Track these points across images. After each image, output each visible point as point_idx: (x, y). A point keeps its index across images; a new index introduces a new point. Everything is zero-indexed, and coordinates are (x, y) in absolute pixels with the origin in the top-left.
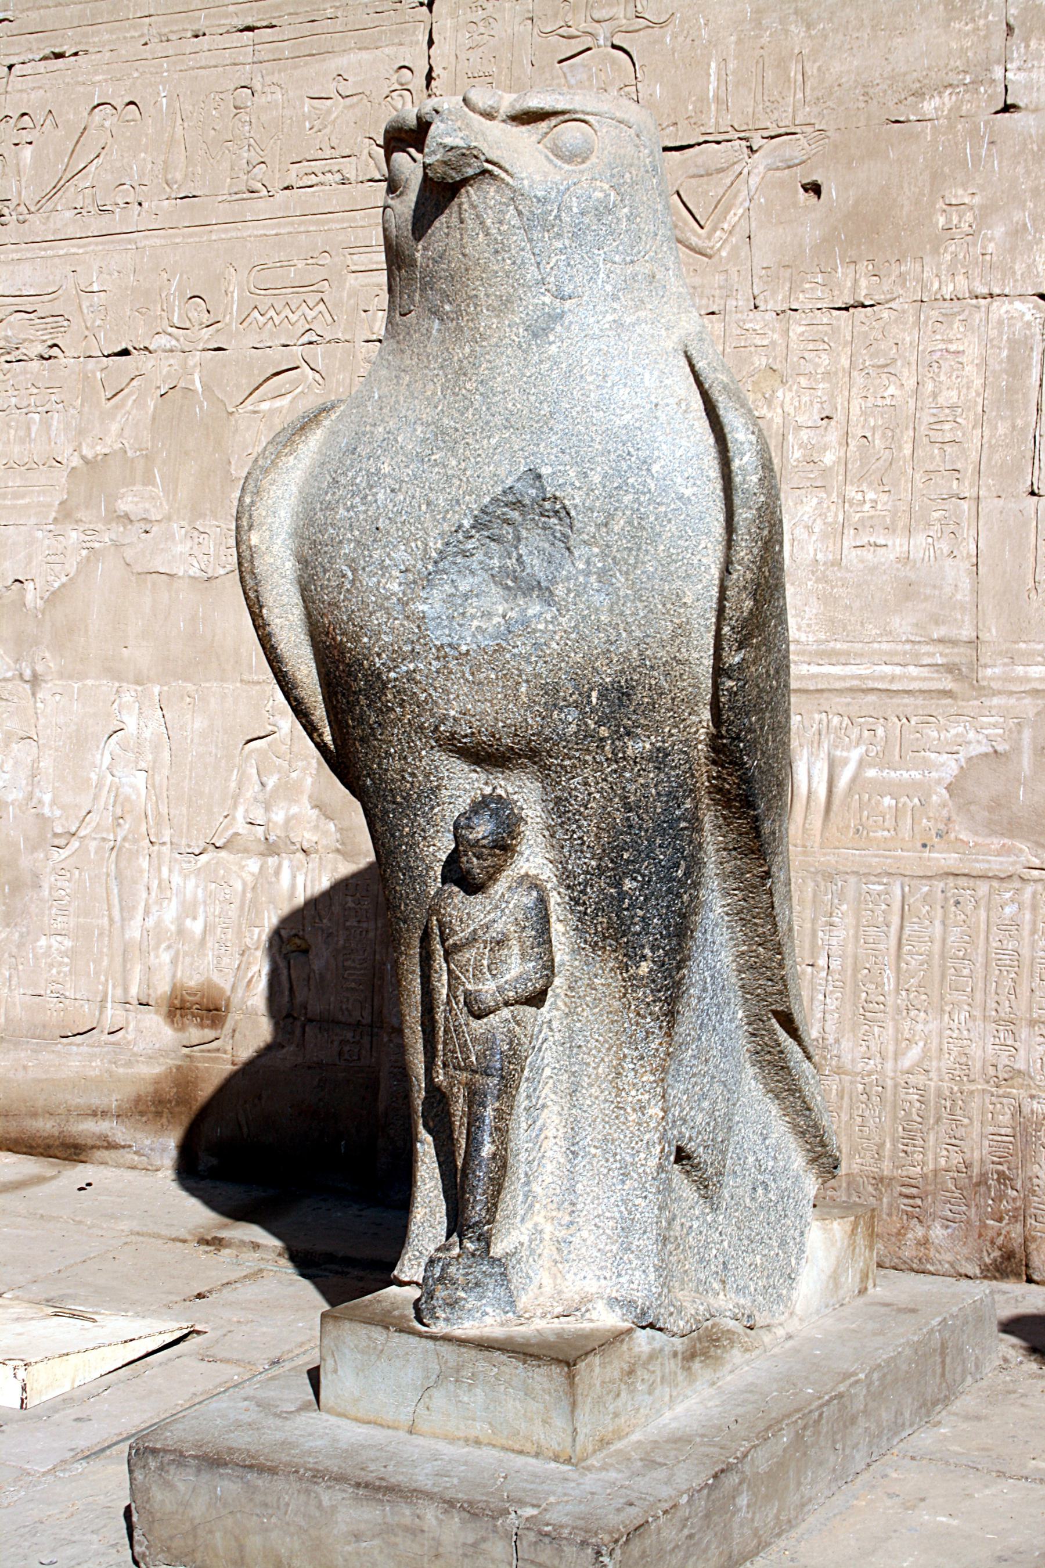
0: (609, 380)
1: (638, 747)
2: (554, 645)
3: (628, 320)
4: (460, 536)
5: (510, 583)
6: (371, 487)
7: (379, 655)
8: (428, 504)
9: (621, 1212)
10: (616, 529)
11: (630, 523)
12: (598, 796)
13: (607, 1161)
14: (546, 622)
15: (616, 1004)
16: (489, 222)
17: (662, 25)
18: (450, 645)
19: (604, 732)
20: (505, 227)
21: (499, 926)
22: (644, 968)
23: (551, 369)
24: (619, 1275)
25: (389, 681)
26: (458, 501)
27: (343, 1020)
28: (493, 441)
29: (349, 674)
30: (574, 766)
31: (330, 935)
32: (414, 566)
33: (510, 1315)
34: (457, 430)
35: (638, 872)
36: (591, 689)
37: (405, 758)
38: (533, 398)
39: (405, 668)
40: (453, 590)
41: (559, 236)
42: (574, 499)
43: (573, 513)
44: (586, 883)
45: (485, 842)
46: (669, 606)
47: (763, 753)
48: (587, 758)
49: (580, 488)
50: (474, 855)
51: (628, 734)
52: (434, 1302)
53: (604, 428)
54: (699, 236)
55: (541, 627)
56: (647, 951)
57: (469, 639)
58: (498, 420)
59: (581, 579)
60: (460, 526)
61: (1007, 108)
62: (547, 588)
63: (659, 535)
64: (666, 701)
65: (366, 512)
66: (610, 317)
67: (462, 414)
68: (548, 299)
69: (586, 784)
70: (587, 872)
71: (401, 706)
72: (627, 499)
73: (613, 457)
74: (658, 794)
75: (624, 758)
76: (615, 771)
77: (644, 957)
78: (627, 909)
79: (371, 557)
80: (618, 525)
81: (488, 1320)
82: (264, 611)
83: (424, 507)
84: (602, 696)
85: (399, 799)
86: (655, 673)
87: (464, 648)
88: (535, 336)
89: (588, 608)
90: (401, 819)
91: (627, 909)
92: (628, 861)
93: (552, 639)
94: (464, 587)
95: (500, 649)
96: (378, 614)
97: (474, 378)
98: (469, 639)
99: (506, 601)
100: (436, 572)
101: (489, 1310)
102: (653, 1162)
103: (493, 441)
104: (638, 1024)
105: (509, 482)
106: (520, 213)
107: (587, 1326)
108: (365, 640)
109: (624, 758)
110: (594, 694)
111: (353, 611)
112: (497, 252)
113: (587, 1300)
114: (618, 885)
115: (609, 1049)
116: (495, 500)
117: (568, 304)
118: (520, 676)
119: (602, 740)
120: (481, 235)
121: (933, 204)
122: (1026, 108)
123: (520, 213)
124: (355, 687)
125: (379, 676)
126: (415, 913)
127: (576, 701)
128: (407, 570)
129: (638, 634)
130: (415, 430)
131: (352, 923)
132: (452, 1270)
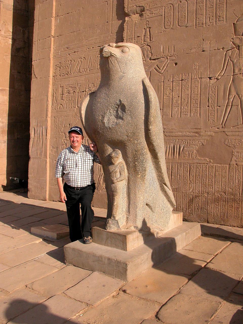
7: (99, 129)
13: (134, 205)
23: (122, 84)
42: (126, 104)
47: (157, 143)
61: (203, 51)
68: (122, 74)
77: (139, 174)
102: (141, 206)
114: (135, 163)
121: (193, 65)
122: (206, 51)
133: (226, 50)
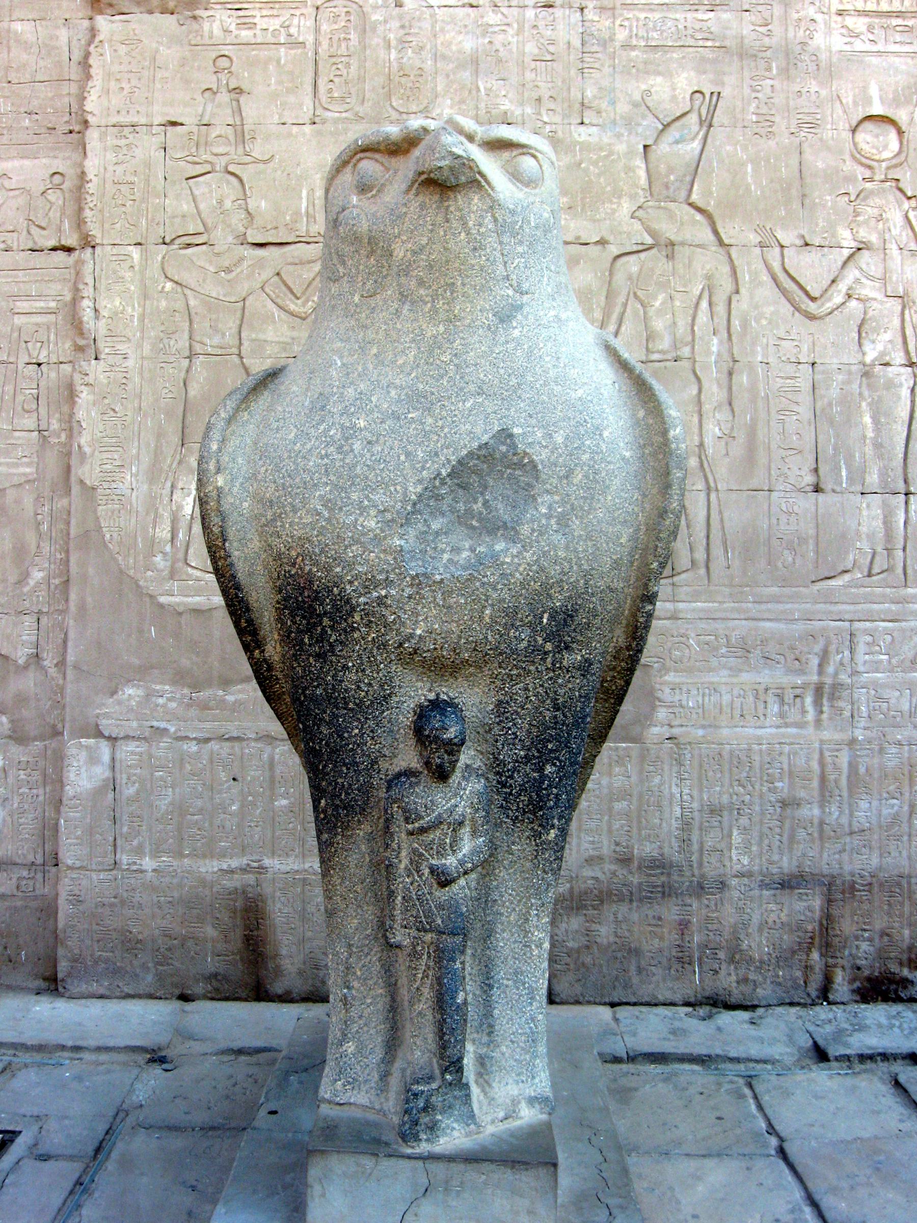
0: (561, 360)
1: (572, 658)
2: (518, 575)
3: (564, 316)
4: (437, 483)
5: (474, 523)
6: (347, 439)
8: (408, 454)
9: (531, 1028)
10: (575, 481)
11: (586, 476)
12: (533, 699)
13: (518, 989)
14: (513, 557)
15: (528, 865)
16: (471, 224)
17: (265, 162)
18: (425, 575)
19: (549, 646)
20: (482, 230)
21: (460, 810)
22: (553, 833)
24: (533, 1078)
25: (359, 605)
26: (436, 454)
27: (20, 862)
28: (468, 405)
29: (316, 598)
30: (519, 675)
31: (6, 799)
32: (394, 507)
33: (472, 1126)
34: (433, 394)
35: (557, 758)
36: (544, 612)
37: (363, 671)
38: (502, 371)
39: (375, 594)
40: (425, 529)
41: (521, 243)
42: (540, 456)
43: (540, 467)
44: (514, 769)
45: (456, 740)
46: (611, 545)
48: (532, 668)
49: (546, 447)
50: (446, 751)
51: (567, 648)
52: (418, 1128)
53: (563, 399)
54: (296, 305)
55: (508, 560)
56: (556, 821)
57: (441, 570)
58: (472, 388)
59: (544, 521)
60: (439, 474)
62: (513, 528)
63: (608, 487)
64: (597, 621)
65: (343, 460)
66: (552, 313)
67: (438, 380)
69: (526, 689)
70: (517, 761)
71: (367, 626)
72: (585, 457)
73: (572, 423)
74: (580, 696)
75: (560, 668)
76: (551, 679)
78: (545, 789)
79: (349, 498)
80: (578, 477)
81: (456, 1134)
82: (227, 544)
83: (403, 458)
84: (552, 617)
85: (351, 705)
86: (594, 599)
87: (438, 577)
88: (502, 321)
89: (549, 545)
90: (350, 723)
91: (545, 789)
92: (551, 751)
93: (517, 570)
94: (435, 525)
95: (471, 579)
96: (354, 548)
97: (449, 351)
98: (441, 570)
99: (471, 538)
100: (413, 513)
101: (455, 1125)
103: (468, 405)
104: (543, 879)
105: (485, 438)
106: (496, 220)
107: (518, 1123)
108: (338, 569)
109: (560, 668)
110: (546, 616)
111: (327, 545)
112: (475, 249)
113: (515, 1102)
114: (541, 770)
115: (519, 901)
116: (471, 454)
117: (525, 298)
118: (487, 601)
119: (546, 653)
120: (463, 234)
123: (496, 220)
124: (319, 609)
125: (348, 601)
126: (356, 801)
127: (530, 622)
128: (385, 511)
129: (585, 567)
130: (389, 392)
131: (24, 790)
132: (434, 1098)
133: (614, 250)
